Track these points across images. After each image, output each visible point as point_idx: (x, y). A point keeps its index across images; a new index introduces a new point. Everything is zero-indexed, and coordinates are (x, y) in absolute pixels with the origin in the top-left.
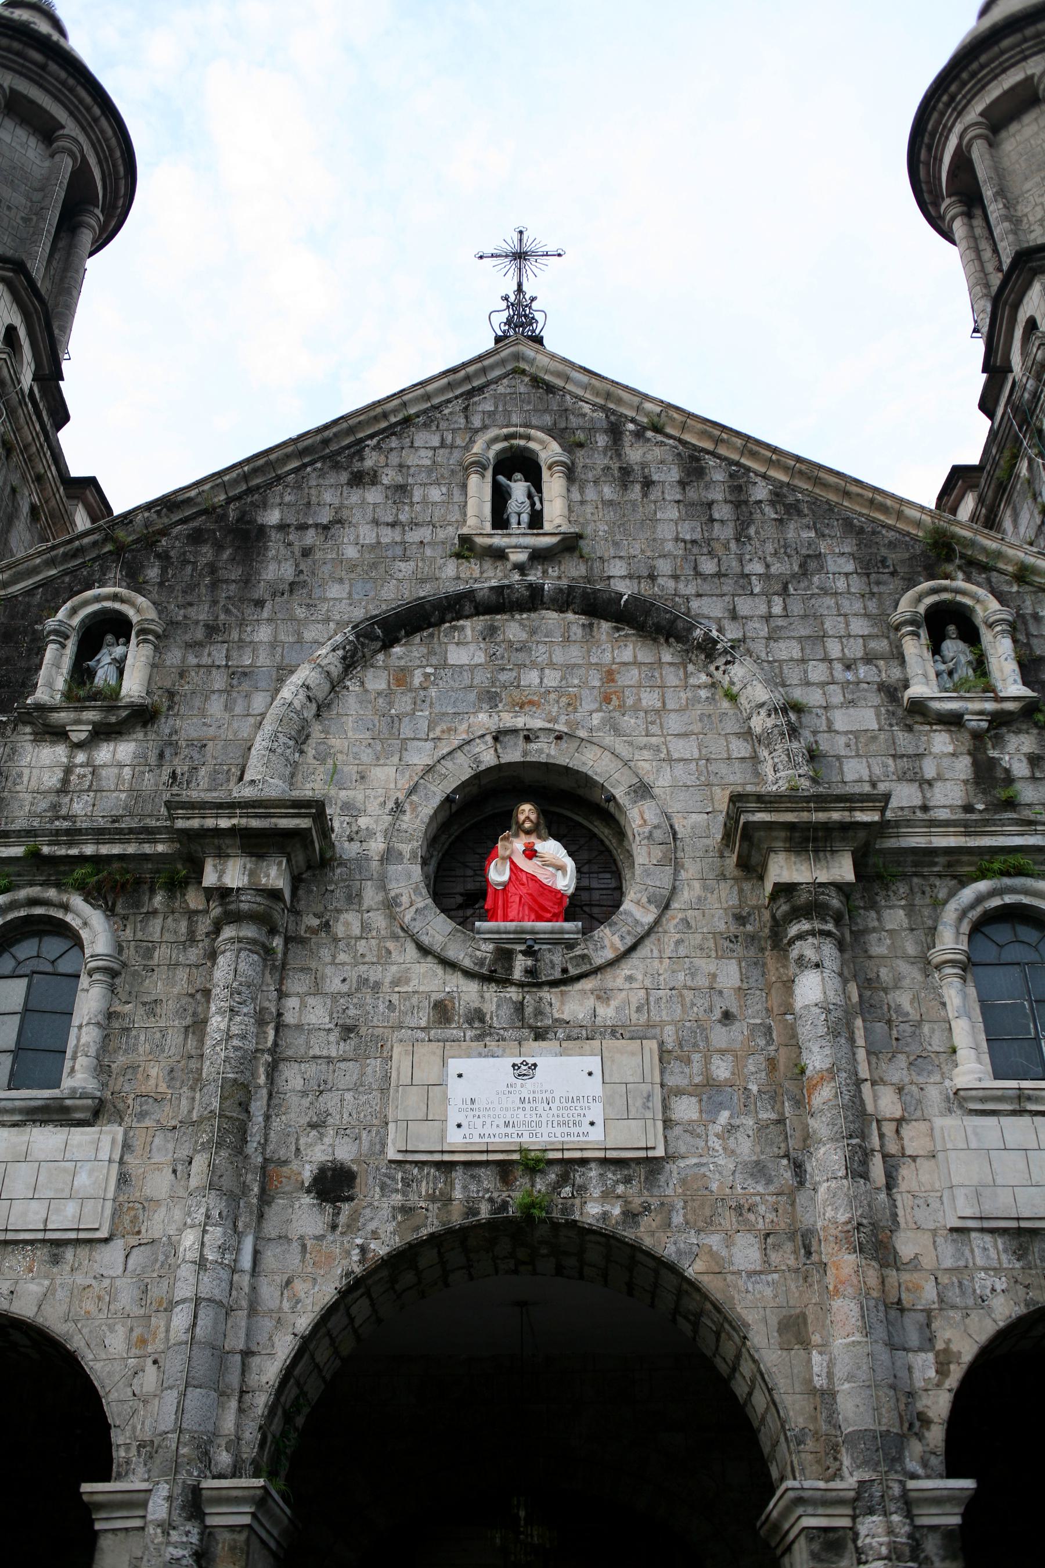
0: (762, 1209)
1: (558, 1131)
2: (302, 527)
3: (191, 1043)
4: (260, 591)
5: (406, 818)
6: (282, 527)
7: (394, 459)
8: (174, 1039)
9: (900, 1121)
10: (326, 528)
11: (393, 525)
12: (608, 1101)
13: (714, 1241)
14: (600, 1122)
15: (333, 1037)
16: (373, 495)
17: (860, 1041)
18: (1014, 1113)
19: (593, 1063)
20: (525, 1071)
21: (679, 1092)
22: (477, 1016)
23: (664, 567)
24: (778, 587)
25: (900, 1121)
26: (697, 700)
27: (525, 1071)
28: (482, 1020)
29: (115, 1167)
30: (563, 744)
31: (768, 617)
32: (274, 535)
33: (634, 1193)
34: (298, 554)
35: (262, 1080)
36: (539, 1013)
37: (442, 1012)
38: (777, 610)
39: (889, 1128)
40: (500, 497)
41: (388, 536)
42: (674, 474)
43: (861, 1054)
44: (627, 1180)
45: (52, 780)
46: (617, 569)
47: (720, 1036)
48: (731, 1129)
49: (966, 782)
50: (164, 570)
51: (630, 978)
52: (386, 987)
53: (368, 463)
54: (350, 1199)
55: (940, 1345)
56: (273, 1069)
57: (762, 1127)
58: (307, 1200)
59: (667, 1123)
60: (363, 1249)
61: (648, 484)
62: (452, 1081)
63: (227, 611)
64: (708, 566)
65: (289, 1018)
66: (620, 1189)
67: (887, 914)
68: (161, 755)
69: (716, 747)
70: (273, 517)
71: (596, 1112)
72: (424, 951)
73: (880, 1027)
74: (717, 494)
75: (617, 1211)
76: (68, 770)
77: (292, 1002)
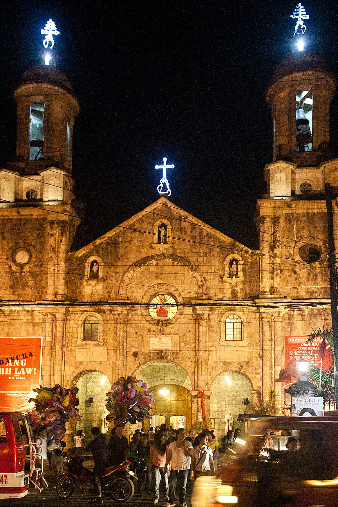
0: (191, 358)
1: (165, 348)
2: (125, 242)
3: (115, 335)
4: (119, 256)
5: (144, 299)
6: (122, 242)
7: (140, 225)
8: (113, 334)
9: (211, 347)
10: (129, 242)
11: (140, 241)
12: (172, 344)
13: (184, 362)
14: (170, 347)
15: (135, 334)
16: (137, 234)
17: (207, 336)
18: (227, 346)
19: (170, 338)
20: (161, 339)
21: (181, 342)
22: (154, 331)
23: (187, 251)
24: (205, 255)
25: (211, 347)
26: (190, 277)
27: (161, 339)
28: (155, 332)
29: (107, 352)
30: (168, 286)
31: (203, 262)
32: (120, 243)
33: (175, 356)
34: (125, 248)
35: (125, 340)
36: (163, 331)
37: (149, 330)
38: (205, 260)
39: (209, 348)
40: (159, 232)
41: (140, 244)
42: (190, 229)
43: (207, 338)
44: (174, 354)
45: (90, 292)
46: (178, 251)
47: (188, 334)
48: (188, 348)
49: (230, 293)
50: (103, 251)
51: (176, 326)
52: (142, 327)
53: (136, 227)
54: (137, 356)
55: (211, 375)
56: (126, 339)
57: (192, 348)
58: (132, 356)
59: (180, 347)
60: (140, 363)
61: (185, 232)
62: (151, 341)
63: (114, 260)
64: (194, 251)
65: (128, 331)
66: (173, 355)
67: (214, 315)
68: (106, 288)
69: (192, 287)
70: (120, 239)
71: (170, 345)
72: (147, 321)
73: (211, 334)
74: (197, 235)
75: (172, 358)
76: (92, 291)
77: (128, 329)
